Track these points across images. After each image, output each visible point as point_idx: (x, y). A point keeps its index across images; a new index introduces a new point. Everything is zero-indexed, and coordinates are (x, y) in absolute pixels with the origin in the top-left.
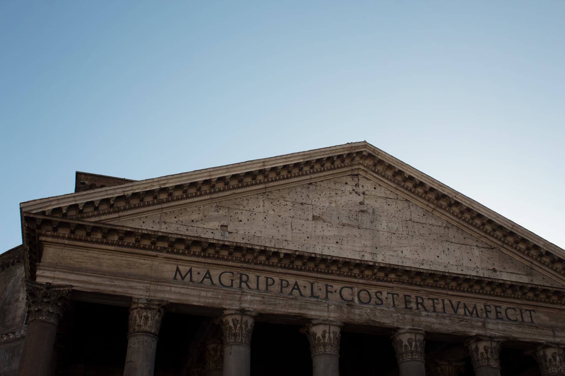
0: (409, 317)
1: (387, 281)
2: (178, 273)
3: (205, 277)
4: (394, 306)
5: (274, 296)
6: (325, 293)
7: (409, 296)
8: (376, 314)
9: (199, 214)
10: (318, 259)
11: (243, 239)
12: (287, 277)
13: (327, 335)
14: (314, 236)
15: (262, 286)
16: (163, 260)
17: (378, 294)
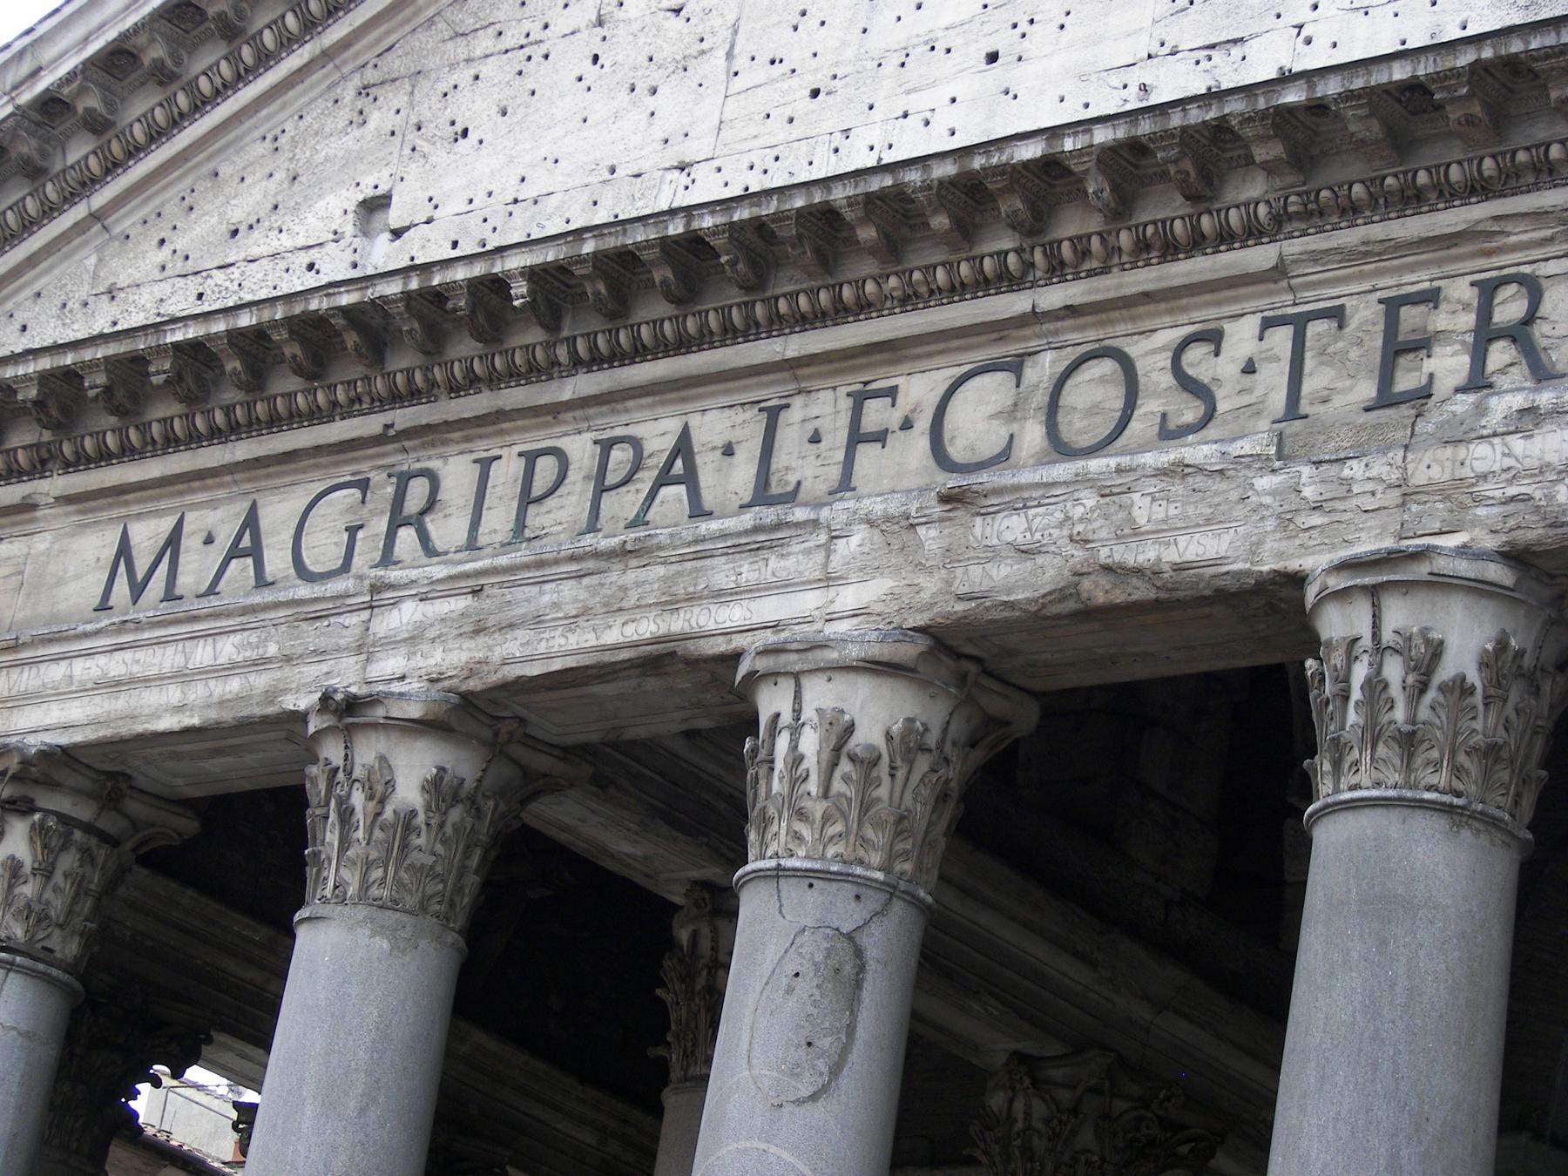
0: (1379, 468)
1: (1225, 239)
2: (122, 568)
3: (234, 553)
4: (1293, 410)
5: (526, 566)
6: (840, 455)
7: (1431, 298)
8: (1136, 513)
9: (271, 175)
10: (715, 242)
11: (455, 244)
12: (637, 416)
13: (782, 743)
14: (849, 69)
15: (498, 520)
16: (67, 515)
17: (1196, 357)
